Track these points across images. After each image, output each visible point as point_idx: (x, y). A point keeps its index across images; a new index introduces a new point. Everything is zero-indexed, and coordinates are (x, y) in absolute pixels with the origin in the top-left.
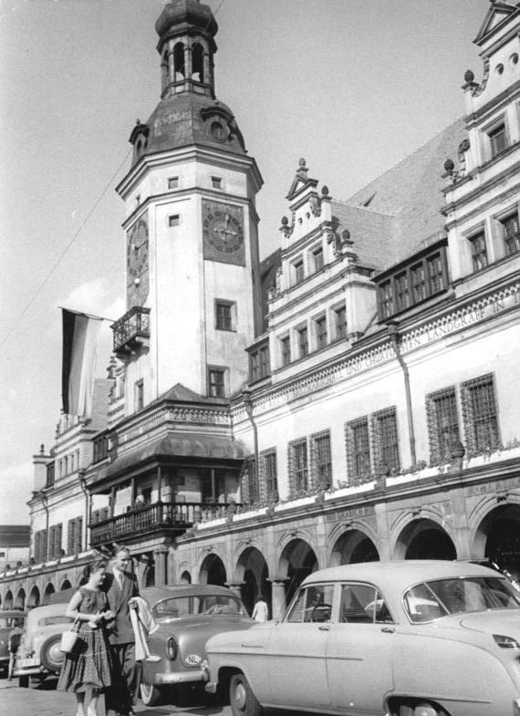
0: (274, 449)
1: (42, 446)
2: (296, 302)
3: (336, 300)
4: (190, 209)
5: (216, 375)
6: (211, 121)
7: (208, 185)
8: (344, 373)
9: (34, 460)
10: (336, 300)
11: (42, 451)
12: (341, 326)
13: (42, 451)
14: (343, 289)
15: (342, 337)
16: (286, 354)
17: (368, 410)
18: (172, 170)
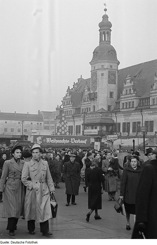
0: (120, 123)
1: (58, 105)
2: (126, 98)
3: (133, 100)
4: (106, 73)
5: (109, 107)
6: (110, 53)
7: (109, 67)
8: (133, 113)
9: (56, 109)
10: (133, 100)
11: (58, 107)
12: (133, 105)
13: (58, 107)
14: (134, 99)
15: (133, 107)
16: (123, 106)
17: (136, 121)
18: (103, 64)
